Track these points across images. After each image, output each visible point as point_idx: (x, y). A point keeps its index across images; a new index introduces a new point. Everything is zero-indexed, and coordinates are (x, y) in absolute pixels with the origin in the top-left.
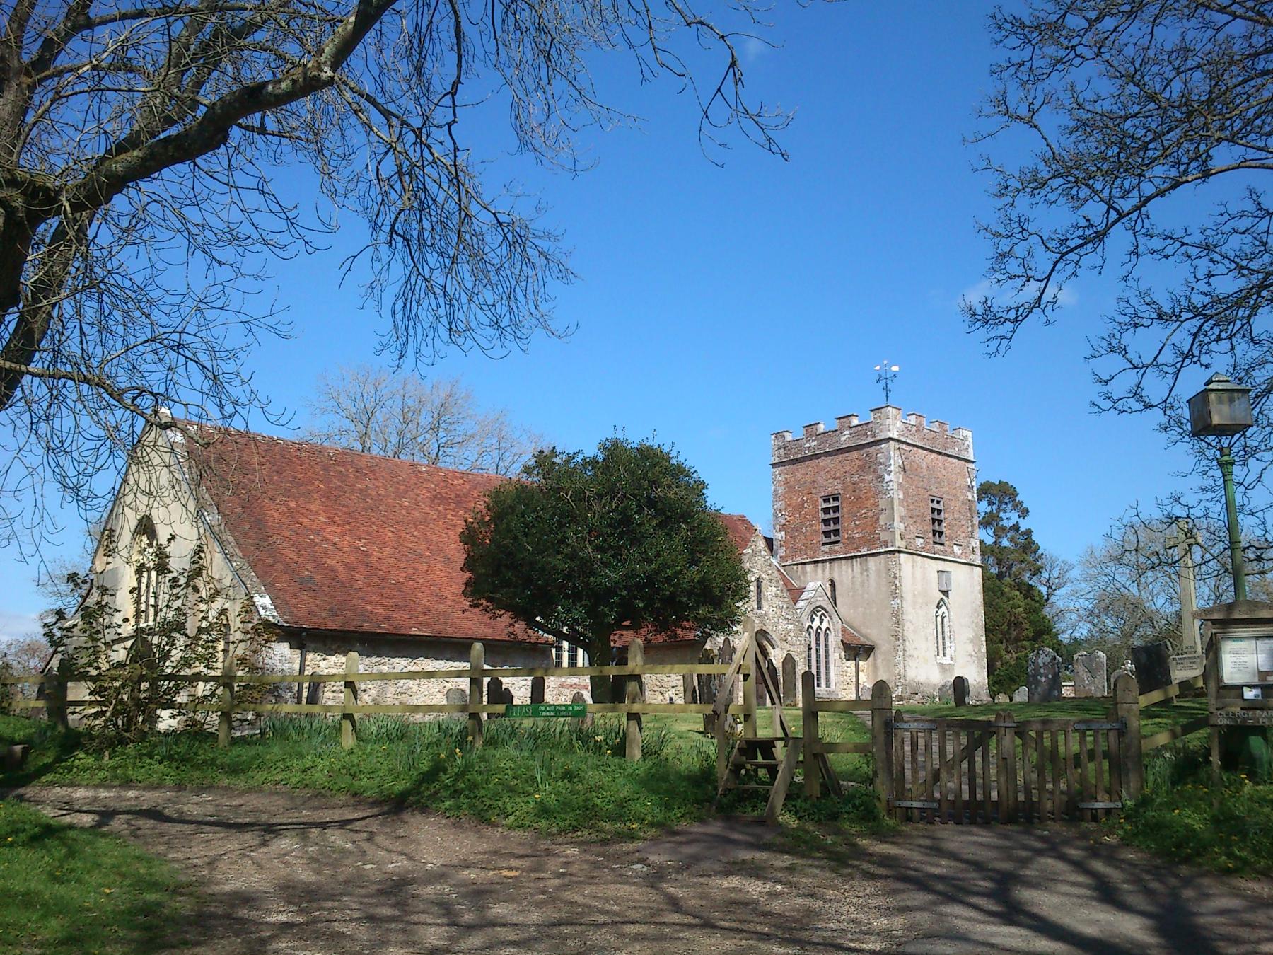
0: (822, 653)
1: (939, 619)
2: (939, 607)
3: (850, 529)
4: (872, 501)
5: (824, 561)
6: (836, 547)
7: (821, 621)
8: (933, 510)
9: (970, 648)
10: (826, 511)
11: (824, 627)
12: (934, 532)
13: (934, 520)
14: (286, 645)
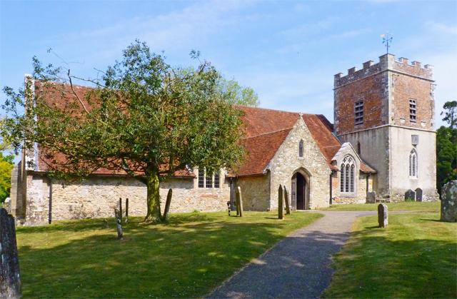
0: (349, 176)
1: (412, 158)
2: (412, 152)
3: (368, 116)
4: (378, 102)
5: (355, 133)
6: (361, 126)
7: (349, 161)
8: (411, 105)
9: (428, 172)
10: (357, 109)
11: (351, 164)
12: (411, 116)
13: (411, 111)
14: (41, 181)
